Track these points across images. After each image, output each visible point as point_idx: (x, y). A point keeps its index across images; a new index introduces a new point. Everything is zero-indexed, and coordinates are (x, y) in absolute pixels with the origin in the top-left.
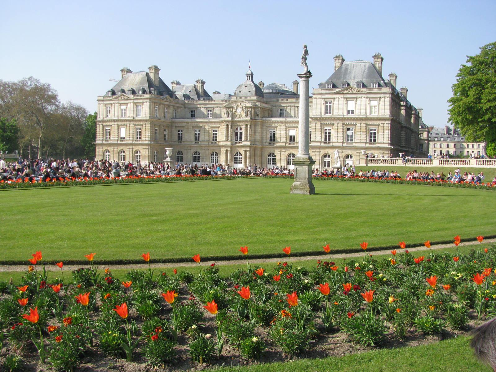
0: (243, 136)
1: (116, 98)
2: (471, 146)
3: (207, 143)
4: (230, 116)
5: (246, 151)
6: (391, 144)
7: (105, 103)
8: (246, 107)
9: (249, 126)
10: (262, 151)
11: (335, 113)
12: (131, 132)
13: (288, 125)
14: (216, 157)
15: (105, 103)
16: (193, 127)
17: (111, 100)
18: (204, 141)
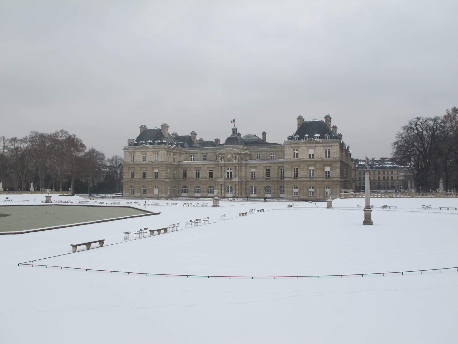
0: (233, 174)
1: (139, 148)
2: (386, 173)
3: (205, 180)
5: (235, 185)
6: (340, 178)
9: (237, 167)
10: (246, 184)
11: (300, 157)
15: (129, 151)
16: (194, 168)
18: (203, 178)
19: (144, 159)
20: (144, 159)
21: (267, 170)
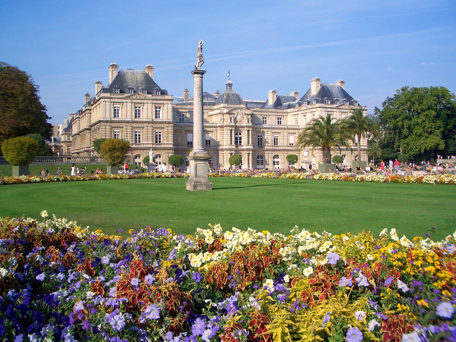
1: (129, 96)
7: (112, 100)
8: (246, 114)
12: (150, 135)
13: (273, 131)
14: (261, 160)
17: (123, 98)
19: (137, 114)
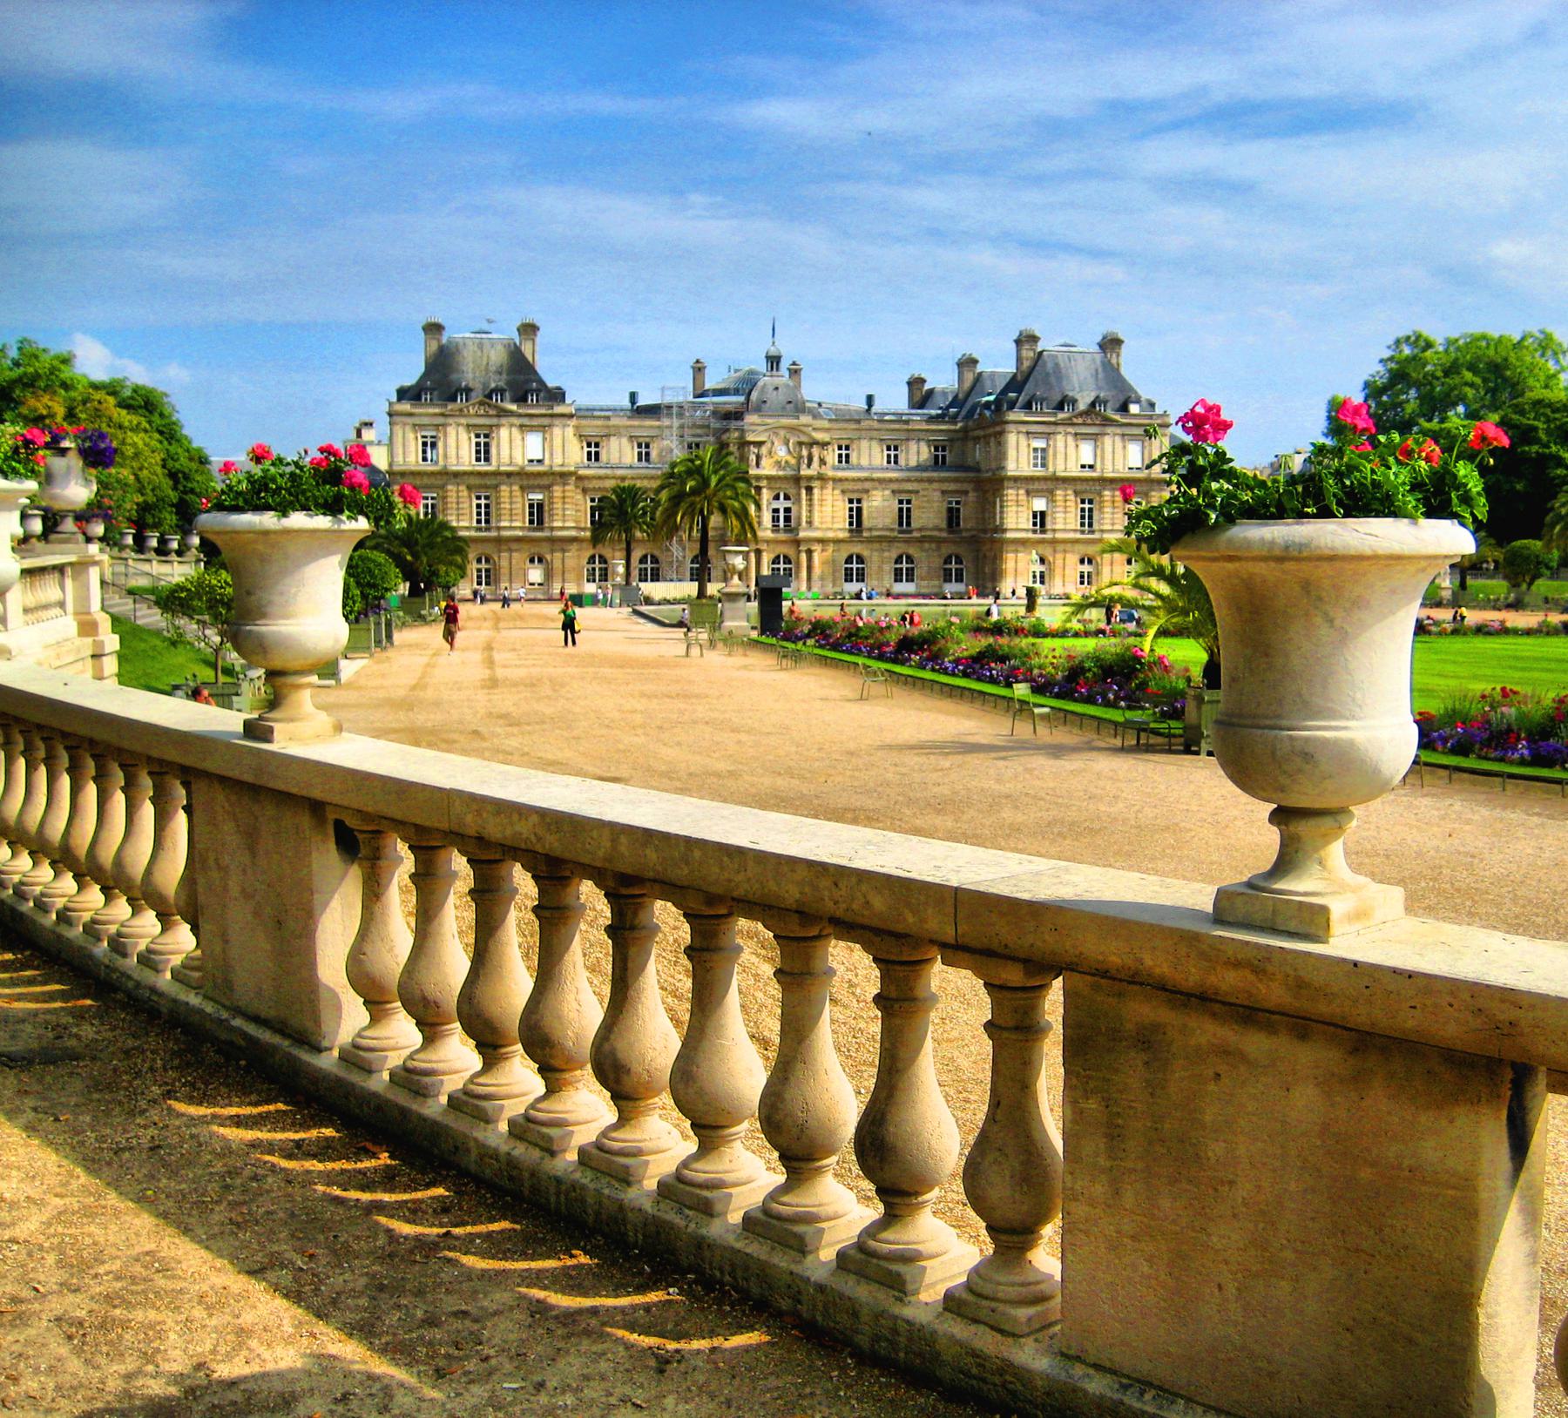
4: (764, 462)
7: (417, 421)
9: (816, 491)
17: (443, 415)
19: (483, 452)
20: (483, 452)
21: (901, 502)
